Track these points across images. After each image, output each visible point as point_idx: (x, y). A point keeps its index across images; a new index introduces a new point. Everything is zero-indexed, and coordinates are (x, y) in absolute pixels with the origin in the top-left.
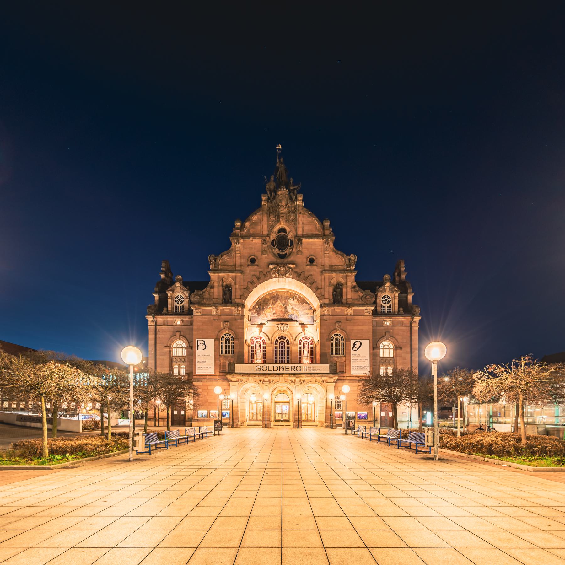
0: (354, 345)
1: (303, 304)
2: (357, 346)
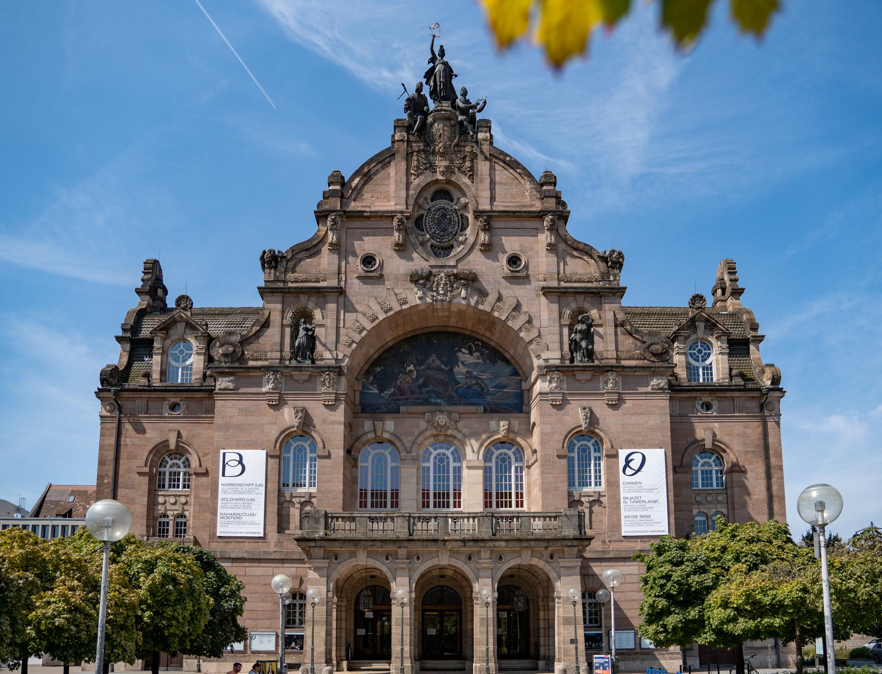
0: (628, 462)
2: (635, 464)
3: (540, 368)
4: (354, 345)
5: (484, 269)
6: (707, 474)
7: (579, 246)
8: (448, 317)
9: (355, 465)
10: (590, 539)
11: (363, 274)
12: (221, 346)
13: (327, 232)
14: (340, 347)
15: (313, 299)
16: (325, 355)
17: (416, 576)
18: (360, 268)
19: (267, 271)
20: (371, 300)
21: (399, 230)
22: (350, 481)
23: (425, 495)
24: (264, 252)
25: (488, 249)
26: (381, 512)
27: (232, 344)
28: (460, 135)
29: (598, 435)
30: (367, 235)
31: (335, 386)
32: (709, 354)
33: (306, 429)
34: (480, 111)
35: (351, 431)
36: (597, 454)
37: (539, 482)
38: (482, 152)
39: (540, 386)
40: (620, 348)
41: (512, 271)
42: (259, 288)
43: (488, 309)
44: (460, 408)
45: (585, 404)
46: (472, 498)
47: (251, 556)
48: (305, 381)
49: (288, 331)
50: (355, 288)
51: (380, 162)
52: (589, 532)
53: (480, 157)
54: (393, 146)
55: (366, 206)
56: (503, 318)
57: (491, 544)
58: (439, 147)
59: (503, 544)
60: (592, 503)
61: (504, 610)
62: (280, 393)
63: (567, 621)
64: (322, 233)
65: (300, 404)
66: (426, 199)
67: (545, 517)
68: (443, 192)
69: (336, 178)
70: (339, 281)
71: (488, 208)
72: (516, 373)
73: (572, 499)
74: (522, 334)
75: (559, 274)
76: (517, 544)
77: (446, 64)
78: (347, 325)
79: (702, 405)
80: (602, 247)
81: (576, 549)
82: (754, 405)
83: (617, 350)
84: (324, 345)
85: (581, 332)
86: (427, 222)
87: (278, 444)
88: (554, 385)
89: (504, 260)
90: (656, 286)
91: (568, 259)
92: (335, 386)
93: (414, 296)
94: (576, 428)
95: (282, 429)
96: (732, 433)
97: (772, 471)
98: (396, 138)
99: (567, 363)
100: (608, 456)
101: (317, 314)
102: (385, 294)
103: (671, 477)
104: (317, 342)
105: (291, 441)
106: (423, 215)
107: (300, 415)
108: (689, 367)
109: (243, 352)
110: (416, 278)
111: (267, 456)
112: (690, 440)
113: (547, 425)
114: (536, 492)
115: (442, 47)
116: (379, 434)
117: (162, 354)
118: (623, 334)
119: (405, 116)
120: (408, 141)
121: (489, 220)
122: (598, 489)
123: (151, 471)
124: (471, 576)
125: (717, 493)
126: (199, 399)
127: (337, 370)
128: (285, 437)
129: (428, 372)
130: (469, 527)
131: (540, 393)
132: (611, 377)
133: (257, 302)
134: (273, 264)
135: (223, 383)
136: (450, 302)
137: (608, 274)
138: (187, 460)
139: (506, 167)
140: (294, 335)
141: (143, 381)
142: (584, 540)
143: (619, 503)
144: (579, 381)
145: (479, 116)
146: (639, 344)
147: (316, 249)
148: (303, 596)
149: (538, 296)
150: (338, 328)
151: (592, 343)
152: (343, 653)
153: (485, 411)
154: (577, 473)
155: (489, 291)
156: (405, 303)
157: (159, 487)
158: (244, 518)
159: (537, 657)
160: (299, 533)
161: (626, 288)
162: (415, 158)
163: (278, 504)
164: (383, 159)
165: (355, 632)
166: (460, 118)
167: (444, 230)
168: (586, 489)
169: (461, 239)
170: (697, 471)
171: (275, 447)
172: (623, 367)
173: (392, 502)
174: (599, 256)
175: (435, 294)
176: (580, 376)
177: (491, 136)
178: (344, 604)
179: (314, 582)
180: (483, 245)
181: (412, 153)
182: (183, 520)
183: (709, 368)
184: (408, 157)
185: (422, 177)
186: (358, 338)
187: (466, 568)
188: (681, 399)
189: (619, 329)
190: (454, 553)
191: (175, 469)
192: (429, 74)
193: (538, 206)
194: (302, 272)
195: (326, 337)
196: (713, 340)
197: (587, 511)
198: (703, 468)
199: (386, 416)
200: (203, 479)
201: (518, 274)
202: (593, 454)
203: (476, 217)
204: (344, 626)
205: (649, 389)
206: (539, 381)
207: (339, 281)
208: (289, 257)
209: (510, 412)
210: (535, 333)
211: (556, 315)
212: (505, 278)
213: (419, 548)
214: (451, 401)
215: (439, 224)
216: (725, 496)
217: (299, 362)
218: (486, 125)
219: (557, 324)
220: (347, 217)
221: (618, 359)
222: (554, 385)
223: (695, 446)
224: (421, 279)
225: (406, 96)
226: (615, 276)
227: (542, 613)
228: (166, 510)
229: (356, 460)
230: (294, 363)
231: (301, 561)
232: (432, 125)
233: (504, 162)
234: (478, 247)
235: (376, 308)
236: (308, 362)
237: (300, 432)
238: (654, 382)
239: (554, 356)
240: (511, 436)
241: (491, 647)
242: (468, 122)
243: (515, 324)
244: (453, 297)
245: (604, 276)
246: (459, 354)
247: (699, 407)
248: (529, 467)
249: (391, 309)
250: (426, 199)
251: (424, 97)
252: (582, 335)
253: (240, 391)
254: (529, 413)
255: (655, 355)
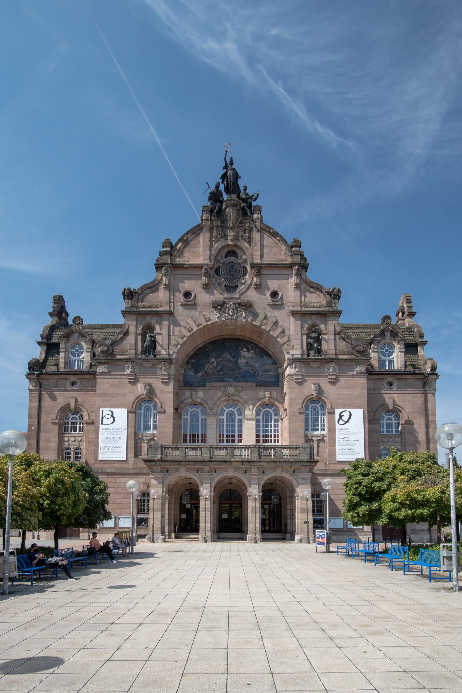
0: (341, 416)
1: (262, 356)
2: (345, 418)
3: (289, 359)
4: (179, 346)
5: (256, 299)
6: (389, 425)
7: (314, 285)
8: (235, 329)
9: (180, 418)
10: (317, 462)
11: (184, 303)
12: (100, 346)
13: (162, 277)
14: (171, 347)
15: (155, 318)
16: (162, 352)
17: (214, 483)
18: (182, 299)
19: (127, 301)
20: (189, 319)
21: (205, 276)
22: (177, 427)
23: (221, 436)
24: (125, 289)
25: (258, 287)
26: (195, 445)
27: (106, 345)
28: (243, 215)
29: (323, 400)
30: (187, 279)
31: (168, 371)
32: (392, 353)
33: (151, 396)
34: (254, 200)
35: (178, 397)
36: (323, 412)
37: (288, 428)
38: (256, 227)
39: (289, 371)
40: (337, 348)
41: (273, 301)
42: (122, 311)
43: (258, 324)
44: (242, 384)
45: (315, 381)
46: (249, 436)
47: (119, 472)
48: (150, 368)
49: (140, 337)
50: (179, 311)
51: (194, 233)
52: (316, 458)
53: (255, 230)
54: (202, 223)
55: (186, 261)
56: (267, 330)
57: (258, 464)
58: (230, 224)
59: (265, 464)
60: (319, 441)
61: (267, 504)
62: (135, 375)
63: (303, 511)
64: (159, 278)
65: (147, 381)
66: (222, 256)
67: (290, 448)
69: (168, 243)
70: (170, 307)
71: (259, 262)
72: (275, 363)
73: (307, 438)
74: (278, 340)
75: (301, 302)
76: (273, 464)
77: (234, 170)
78: (175, 334)
79: (388, 383)
80: (328, 286)
81: (308, 468)
82: (420, 383)
83: (336, 349)
84: (161, 346)
85: (314, 338)
86: (222, 271)
87: (134, 405)
88: (297, 370)
89: (268, 294)
90: (359, 311)
91: (308, 294)
92: (168, 371)
93: (215, 316)
94: (310, 396)
95: (137, 396)
96: (405, 400)
97: (430, 424)
98: (204, 218)
99: (306, 357)
100: (329, 413)
101: (157, 328)
102: (197, 315)
103: (367, 426)
104: (157, 344)
105: (142, 404)
106: (220, 267)
107: (147, 388)
108: (379, 360)
109: (113, 350)
110: (216, 305)
111: (128, 412)
112: (380, 404)
113: (293, 394)
114: (286, 434)
115: (231, 158)
116: (194, 399)
117: (65, 352)
118: (340, 339)
119: (209, 204)
120: (211, 220)
121: (259, 269)
122: (323, 432)
123: (60, 422)
124: (246, 483)
125: (395, 436)
126: (86, 378)
127: (169, 361)
128: (138, 401)
129: (223, 362)
130: (244, 454)
131: (289, 375)
132: (332, 365)
133: (121, 320)
134: (130, 297)
135: (101, 369)
136: (236, 320)
137: (331, 303)
138: (81, 415)
139: (270, 236)
140: (144, 340)
141: (54, 368)
142: (312, 462)
143: (335, 441)
144: (312, 367)
145: (254, 204)
146: (349, 345)
147: (156, 288)
148: (148, 495)
149: (289, 316)
150: (169, 336)
151: (320, 344)
152: (173, 528)
153: (257, 386)
154: (310, 422)
155: (259, 313)
156: (209, 320)
157: (65, 431)
158: (115, 449)
159: (286, 532)
160: (146, 457)
161: (342, 311)
162: (215, 231)
163: (135, 441)
164: (196, 231)
165: (180, 516)
166: (243, 205)
167: (233, 276)
168: (316, 433)
169: (243, 281)
170: (383, 423)
171: (133, 407)
172: (339, 359)
173: (202, 440)
174: (326, 292)
175: (227, 315)
176: (313, 364)
177: (261, 216)
178: (173, 499)
179: (155, 486)
180: (256, 285)
181: (213, 227)
182: (79, 451)
183: (392, 361)
184: (211, 229)
185: (219, 243)
186: (181, 341)
187: (243, 478)
188: (374, 380)
189: (337, 336)
190: (236, 469)
191: (74, 421)
192: (224, 177)
193: (289, 260)
194: (147, 302)
195: (162, 341)
196: (395, 344)
197: (316, 446)
198: (387, 421)
199: (198, 388)
200: (91, 427)
201: (277, 303)
202: (320, 412)
203: (252, 268)
204: (173, 512)
205: (355, 373)
206: (288, 368)
207: (170, 307)
208: (139, 293)
209: (271, 386)
210: (286, 339)
211: (299, 328)
212: (269, 305)
213: (215, 466)
214: (236, 380)
215: (230, 272)
216: (400, 438)
217: (146, 356)
218: (259, 209)
219: (300, 333)
220: (174, 268)
221: (336, 354)
222: (297, 370)
223: (382, 408)
224: (219, 306)
225: (209, 191)
226: (335, 304)
227: (288, 506)
228: (69, 444)
229: (180, 415)
230: (143, 357)
231: (147, 474)
232: (225, 209)
233: (269, 233)
234: (253, 286)
235: (192, 323)
236: (152, 356)
237: (148, 398)
238: (358, 369)
239: (297, 353)
240: (272, 400)
241: (258, 525)
242: (247, 207)
243: (275, 334)
244: (237, 317)
245: (329, 304)
246: (242, 352)
247: (385, 384)
248: (282, 419)
249: (201, 324)
250: (222, 256)
251: (220, 192)
253: (111, 374)
254: (282, 387)
255: (358, 352)
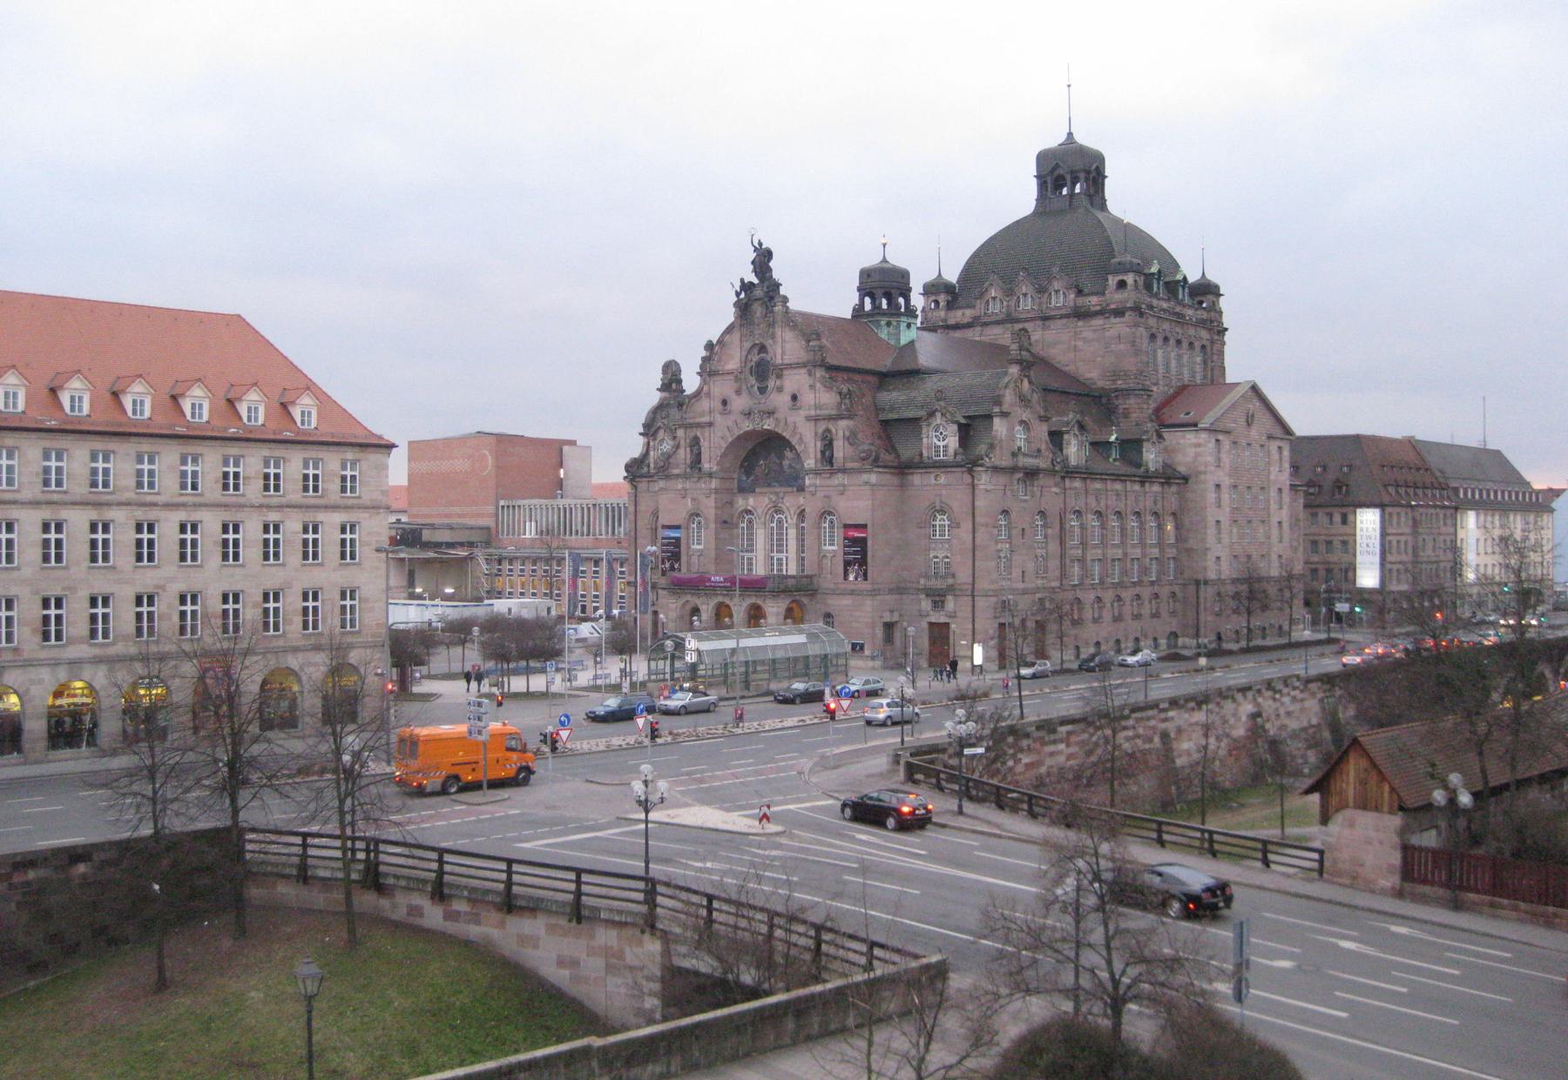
68: (763, 349)
127: (710, 475)
252: (828, 444)
